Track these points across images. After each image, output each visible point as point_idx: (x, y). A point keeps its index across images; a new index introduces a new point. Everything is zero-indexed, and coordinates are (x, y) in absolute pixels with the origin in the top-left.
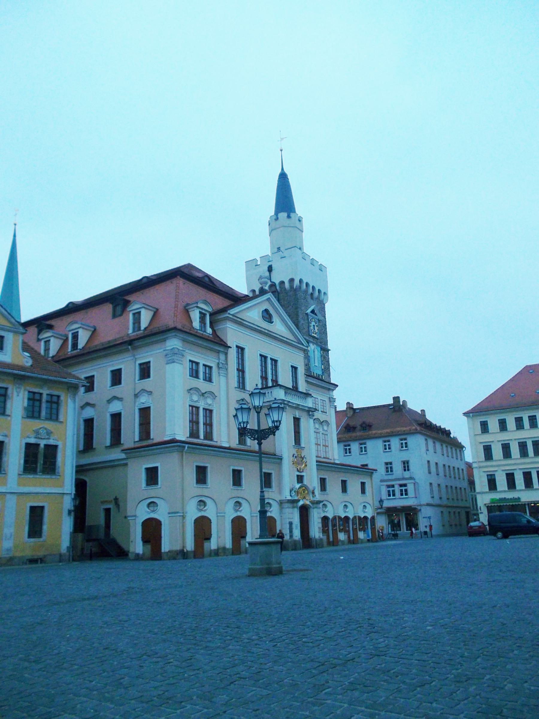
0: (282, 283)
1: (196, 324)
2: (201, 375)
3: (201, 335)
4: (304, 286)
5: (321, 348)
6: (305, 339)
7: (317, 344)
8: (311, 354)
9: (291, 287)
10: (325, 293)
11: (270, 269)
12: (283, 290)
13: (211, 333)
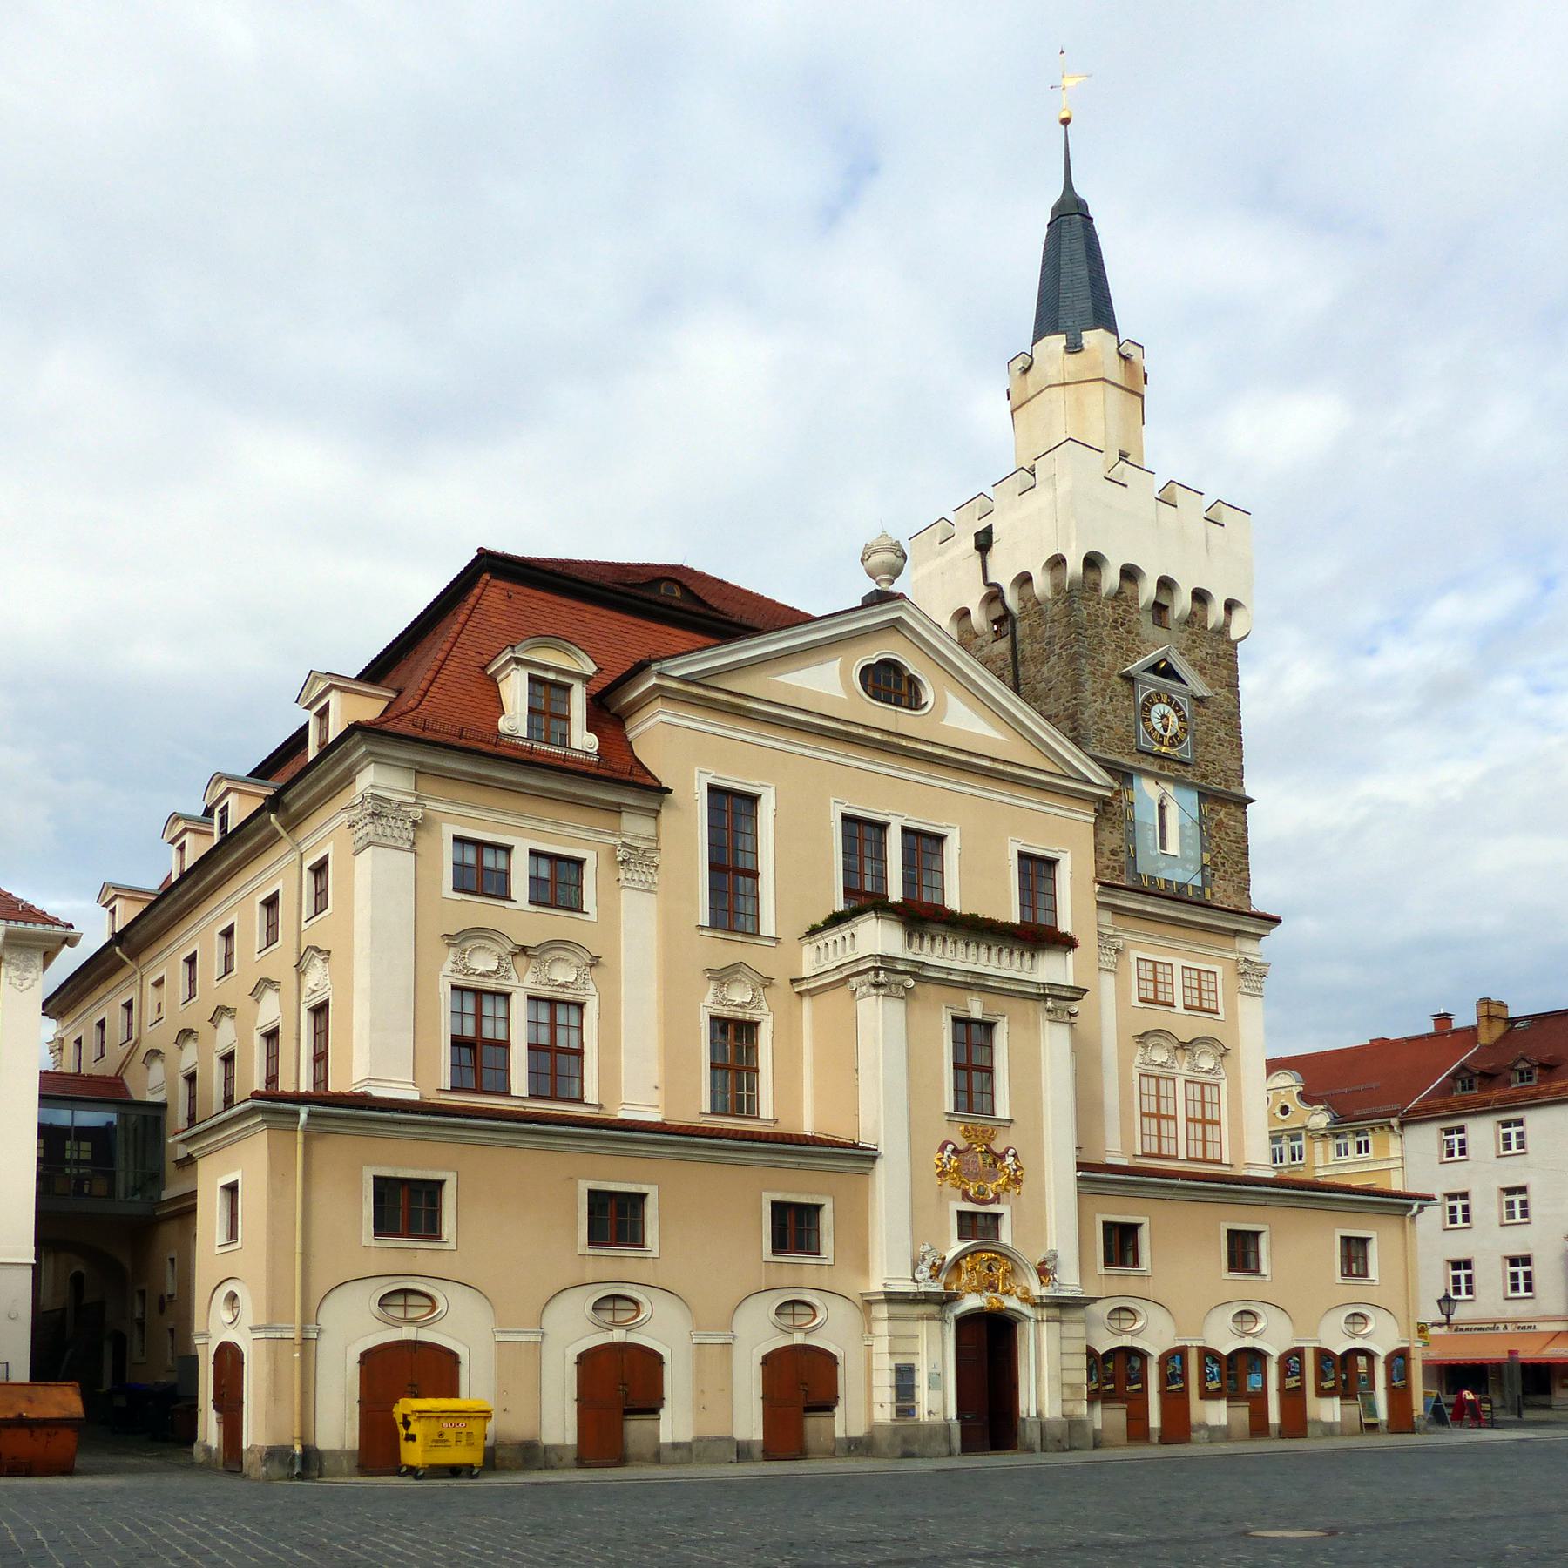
0: (1024, 579)
1: (515, 718)
2: (520, 886)
3: (526, 756)
4: (1111, 578)
5: (1198, 792)
6: (1095, 759)
7: (1178, 782)
8: (1145, 815)
9: (1057, 588)
10: (1230, 606)
11: (984, 542)
12: (1029, 605)
13: (594, 750)
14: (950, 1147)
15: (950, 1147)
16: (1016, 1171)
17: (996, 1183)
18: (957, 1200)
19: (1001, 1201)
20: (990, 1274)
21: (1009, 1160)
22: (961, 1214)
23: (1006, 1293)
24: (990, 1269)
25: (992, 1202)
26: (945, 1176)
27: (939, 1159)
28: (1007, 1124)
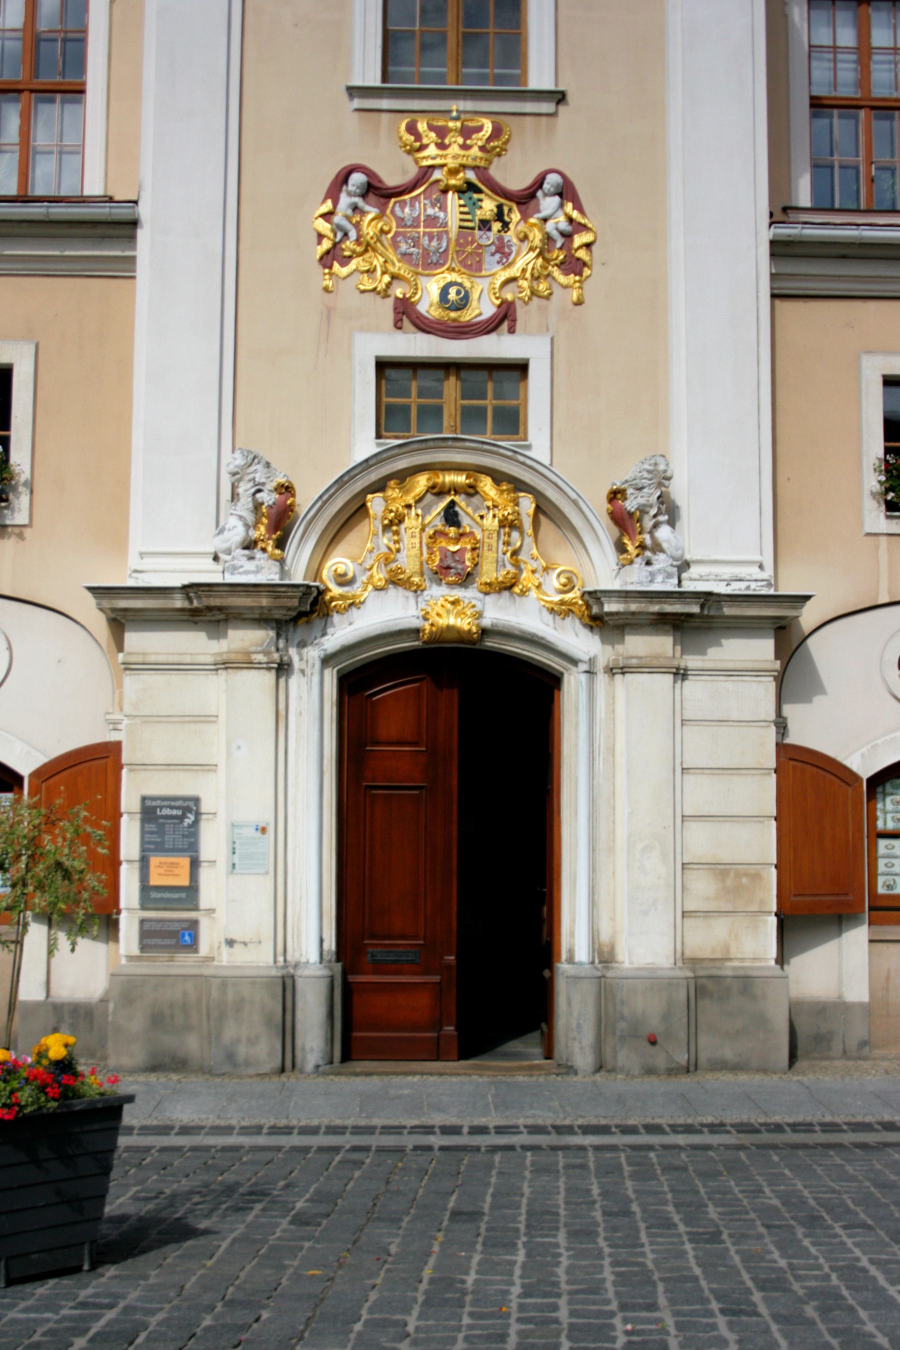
14: (357, 179)
15: (357, 179)
16: (568, 236)
17: (504, 275)
18: (377, 330)
19: (519, 325)
20: (452, 531)
21: (548, 204)
22: (383, 366)
23: (507, 587)
24: (451, 516)
25: (490, 327)
26: (345, 261)
28: (547, 107)
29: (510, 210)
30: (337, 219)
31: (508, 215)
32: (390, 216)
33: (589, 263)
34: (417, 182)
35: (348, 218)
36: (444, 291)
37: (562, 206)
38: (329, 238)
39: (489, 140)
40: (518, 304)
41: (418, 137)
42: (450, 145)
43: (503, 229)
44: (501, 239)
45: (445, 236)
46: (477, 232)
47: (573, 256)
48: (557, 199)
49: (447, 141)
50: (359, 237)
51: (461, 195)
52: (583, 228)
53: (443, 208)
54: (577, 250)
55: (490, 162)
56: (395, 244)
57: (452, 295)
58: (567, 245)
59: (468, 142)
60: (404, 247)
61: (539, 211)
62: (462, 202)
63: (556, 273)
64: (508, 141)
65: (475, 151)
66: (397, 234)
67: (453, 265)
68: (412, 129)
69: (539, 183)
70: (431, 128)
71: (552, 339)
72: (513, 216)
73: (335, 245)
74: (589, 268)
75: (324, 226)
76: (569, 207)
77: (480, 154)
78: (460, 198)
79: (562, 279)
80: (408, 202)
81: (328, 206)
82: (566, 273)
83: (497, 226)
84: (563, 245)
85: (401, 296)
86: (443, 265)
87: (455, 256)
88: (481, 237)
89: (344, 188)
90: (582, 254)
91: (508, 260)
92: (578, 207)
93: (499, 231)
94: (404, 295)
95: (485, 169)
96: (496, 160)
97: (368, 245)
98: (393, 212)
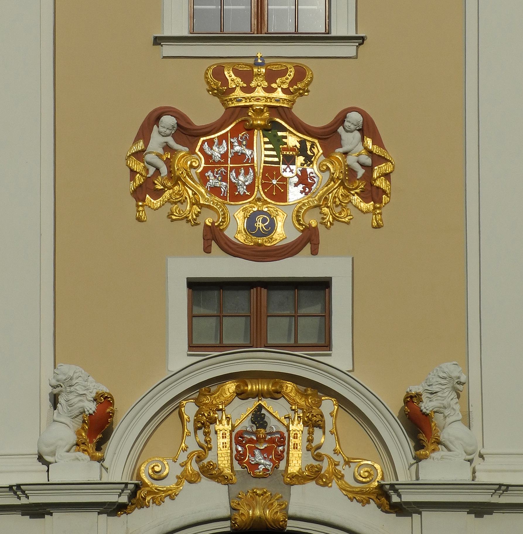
14: (168, 121)
15: (168, 121)
16: (369, 169)
26: (157, 194)
27: (139, 155)
28: (349, 50)
29: (313, 145)
30: (149, 157)
31: (311, 149)
32: (199, 153)
33: (388, 191)
34: (224, 122)
35: (159, 156)
36: (251, 220)
37: (363, 140)
38: (141, 174)
39: (293, 83)
40: (321, 229)
41: (225, 81)
42: (255, 88)
43: (306, 163)
44: (304, 171)
45: (251, 171)
46: (283, 167)
47: (372, 185)
48: (357, 135)
49: (253, 84)
50: (170, 172)
51: (266, 132)
52: (385, 160)
53: (250, 146)
54: (375, 180)
55: (293, 102)
56: (203, 179)
57: (259, 225)
58: (368, 177)
59: (274, 85)
60: (213, 181)
61: (341, 146)
62: (267, 140)
63: (356, 199)
64: (310, 82)
65: (279, 94)
66: (205, 170)
67: (259, 196)
68: (219, 73)
69: (341, 119)
70: (237, 73)
71: (353, 259)
72: (315, 151)
73: (147, 179)
74: (387, 195)
75: (138, 167)
76: (369, 142)
77: (284, 96)
78: (264, 136)
79: (363, 206)
80: (216, 141)
81: (140, 145)
82: (366, 200)
83: (300, 160)
84: (364, 175)
85: (210, 225)
86: (250, 197)
87: (260, 188)
88: (285, 170)
89: (155, 127)
90: (381, 183)
91: (310, 189)
92: (377, 141)
93: (302, 165)
94: (213, 223)
95: (289, 109)
96: (298, 100)
97: (179, 179)
98: (202, 150)
